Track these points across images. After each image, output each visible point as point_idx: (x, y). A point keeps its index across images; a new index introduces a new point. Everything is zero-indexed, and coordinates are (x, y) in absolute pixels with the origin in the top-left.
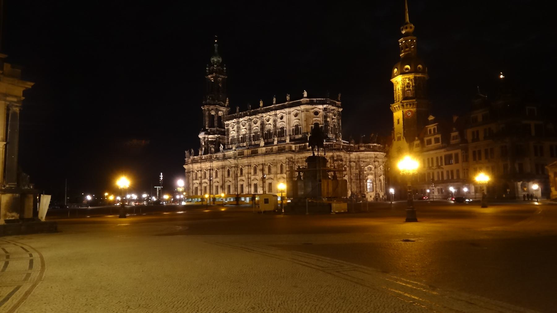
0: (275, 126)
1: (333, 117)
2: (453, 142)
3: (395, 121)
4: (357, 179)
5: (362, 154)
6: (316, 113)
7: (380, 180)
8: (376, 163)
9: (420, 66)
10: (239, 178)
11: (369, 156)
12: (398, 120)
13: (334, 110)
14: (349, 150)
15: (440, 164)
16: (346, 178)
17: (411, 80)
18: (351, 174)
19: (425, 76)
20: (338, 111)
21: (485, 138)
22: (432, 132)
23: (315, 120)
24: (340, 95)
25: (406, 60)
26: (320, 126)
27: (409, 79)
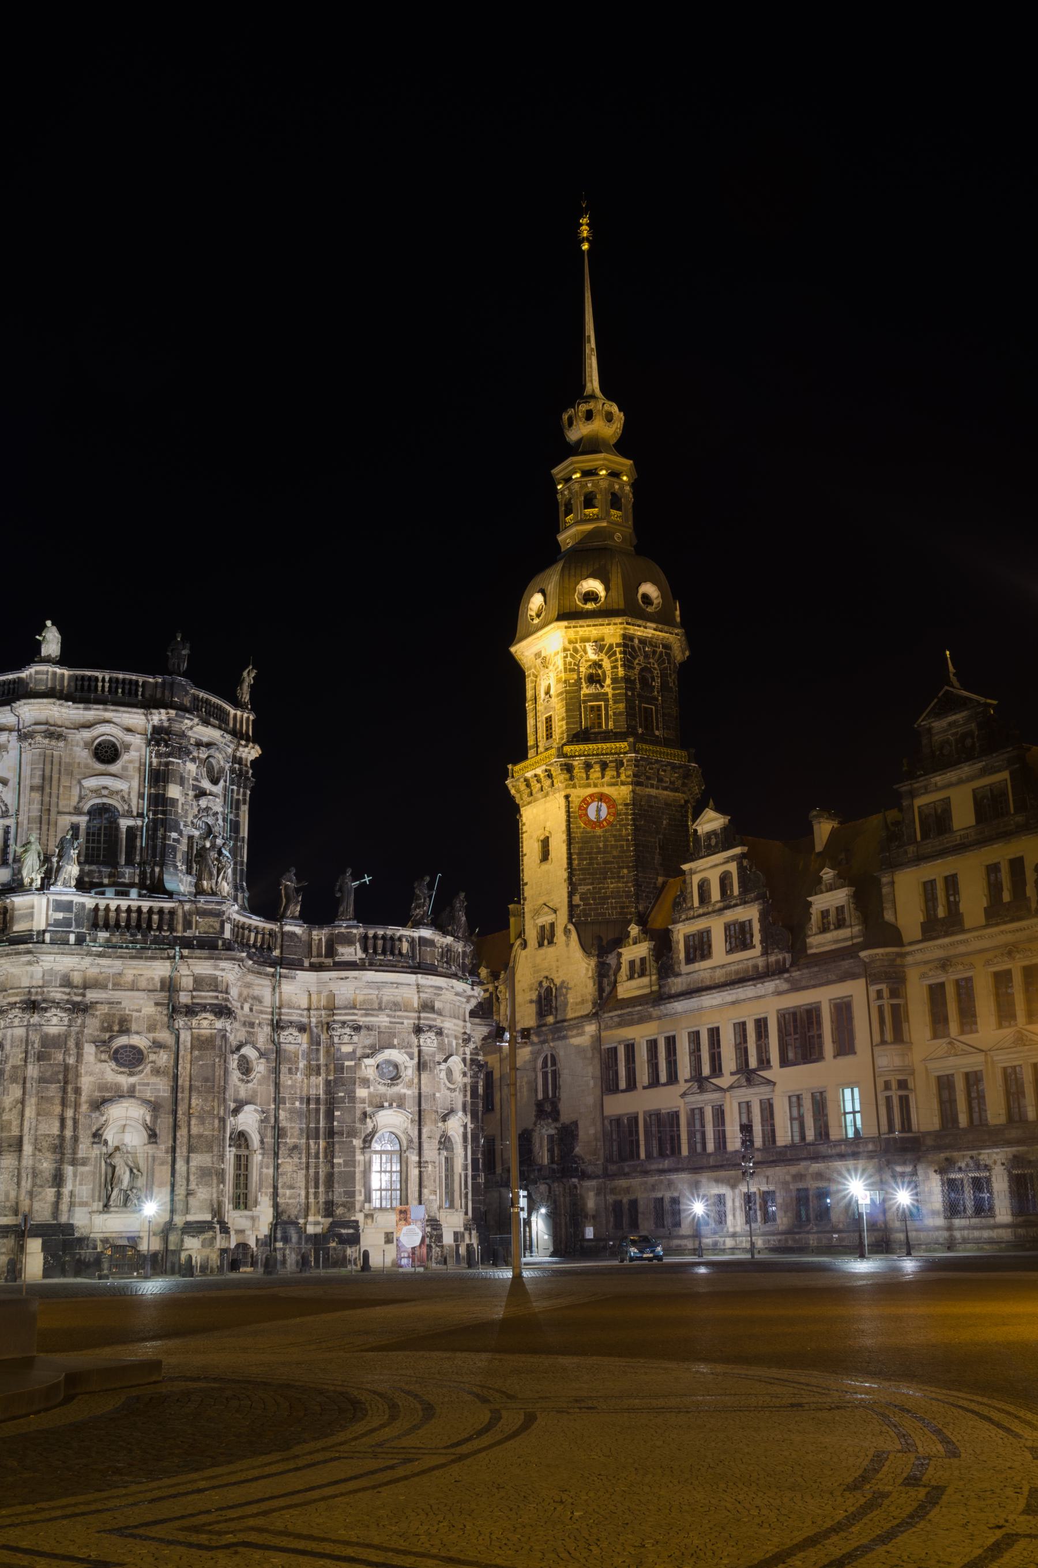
1: (206, 784)
2: (819, 942)
3: (530, 847)
5: (352, 987)
6: (107, 753)
7: (445, 1142)
8: (429, 1042)
9: (648, 589)
11: (389, 995)
12: (545, 843)
13: (209, 745)
14: (273, 957)
16: (248, 1120)
17: (610, 652)
18: (278, 1100)
19: (673, 638)
20: (237, 760)
22: (715, 894)
23: (97, 792)
24: (249, 676)
25: (590, 556)
26: (124, 823)
27: (600, 646)
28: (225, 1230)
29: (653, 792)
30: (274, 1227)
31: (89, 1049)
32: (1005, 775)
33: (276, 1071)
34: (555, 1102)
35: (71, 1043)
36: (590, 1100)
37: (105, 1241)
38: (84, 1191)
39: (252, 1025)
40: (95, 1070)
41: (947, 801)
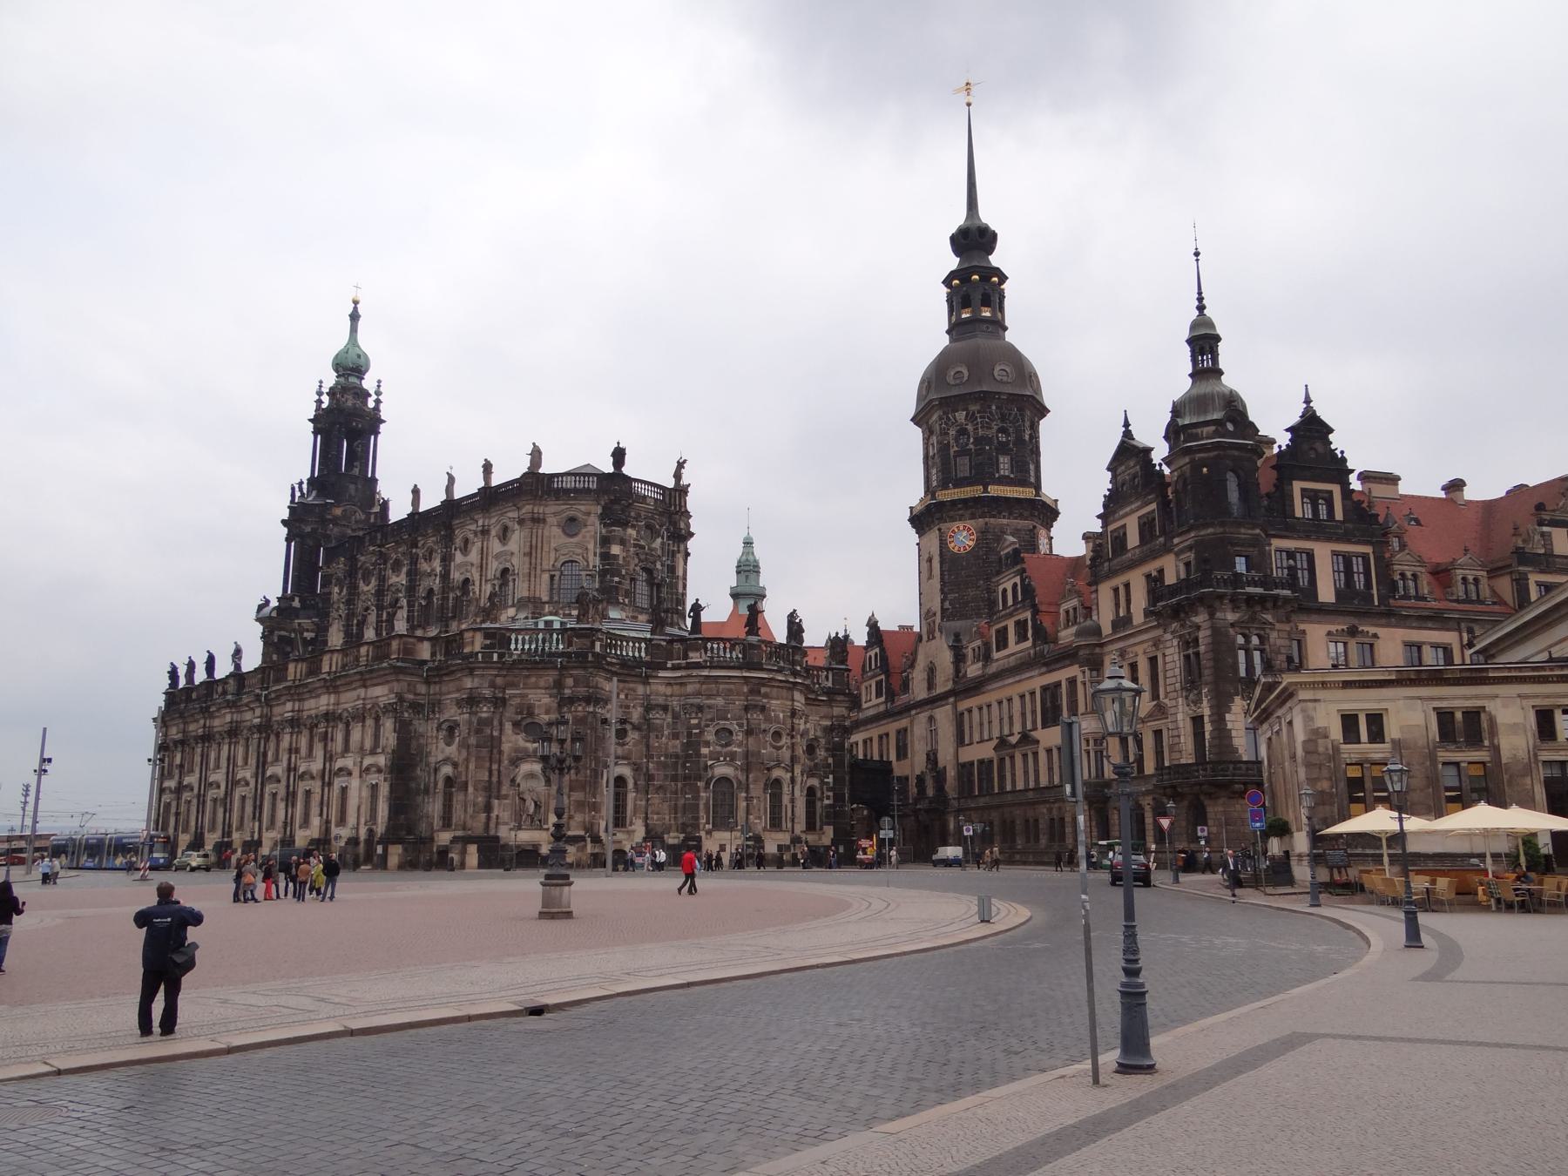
0: (445, 576)
4: (675, 778)
8: (756, 716)
10: (268, 773)
15: (1029, 726)
16: (626, 771)
18: (649, 757)
21: (1147, 613)
22: (1010, 602)
28: (596, 840)
29: (1005, 521)
30: (645, 840)
31: (508, 726)
32: (1153, 506)
33: (647, 737)
34: (935, 754)
35: (496, 723)
36: (952, 750)
37: (518, 847)
38: (505, 815)
39: (628, 707)
40: (513, 740)
41: (1124, 526)
